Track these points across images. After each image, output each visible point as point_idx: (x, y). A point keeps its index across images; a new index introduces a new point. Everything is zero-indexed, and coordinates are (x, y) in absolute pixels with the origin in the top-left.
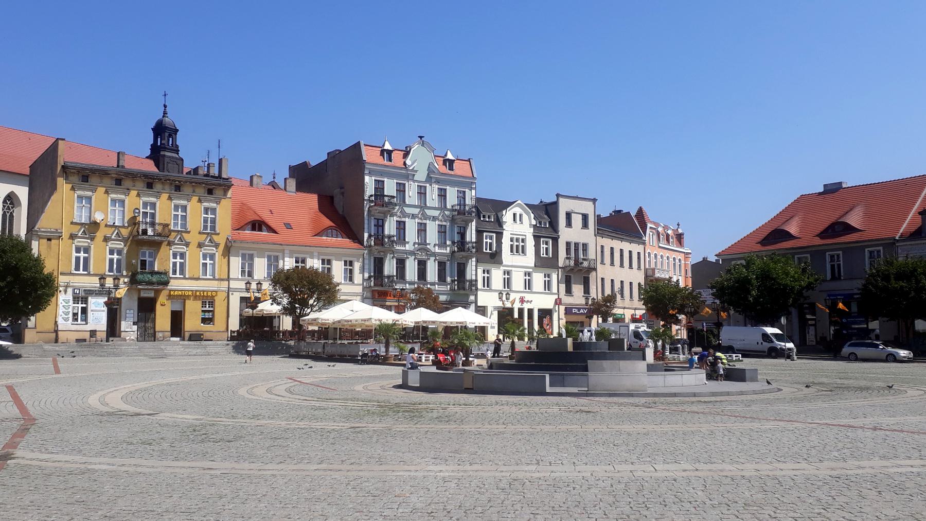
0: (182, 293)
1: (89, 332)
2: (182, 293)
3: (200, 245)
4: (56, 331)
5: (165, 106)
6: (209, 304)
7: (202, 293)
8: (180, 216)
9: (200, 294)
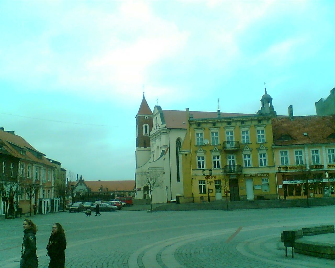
0: (250, 175)
1: (200, 198)
2: (250, 175)
3: (258, 150)
4: (193, 197)
5: (265, 89)
6: (266, 181)
7: (261, 174)
8: (261, 136)
9: (260, 175)
